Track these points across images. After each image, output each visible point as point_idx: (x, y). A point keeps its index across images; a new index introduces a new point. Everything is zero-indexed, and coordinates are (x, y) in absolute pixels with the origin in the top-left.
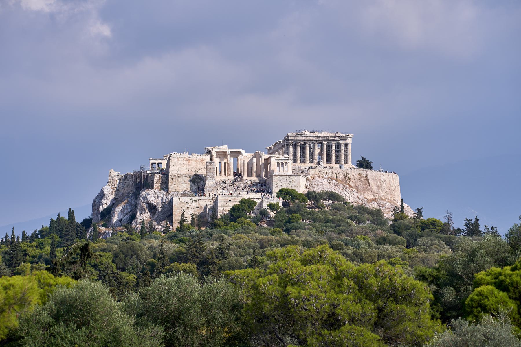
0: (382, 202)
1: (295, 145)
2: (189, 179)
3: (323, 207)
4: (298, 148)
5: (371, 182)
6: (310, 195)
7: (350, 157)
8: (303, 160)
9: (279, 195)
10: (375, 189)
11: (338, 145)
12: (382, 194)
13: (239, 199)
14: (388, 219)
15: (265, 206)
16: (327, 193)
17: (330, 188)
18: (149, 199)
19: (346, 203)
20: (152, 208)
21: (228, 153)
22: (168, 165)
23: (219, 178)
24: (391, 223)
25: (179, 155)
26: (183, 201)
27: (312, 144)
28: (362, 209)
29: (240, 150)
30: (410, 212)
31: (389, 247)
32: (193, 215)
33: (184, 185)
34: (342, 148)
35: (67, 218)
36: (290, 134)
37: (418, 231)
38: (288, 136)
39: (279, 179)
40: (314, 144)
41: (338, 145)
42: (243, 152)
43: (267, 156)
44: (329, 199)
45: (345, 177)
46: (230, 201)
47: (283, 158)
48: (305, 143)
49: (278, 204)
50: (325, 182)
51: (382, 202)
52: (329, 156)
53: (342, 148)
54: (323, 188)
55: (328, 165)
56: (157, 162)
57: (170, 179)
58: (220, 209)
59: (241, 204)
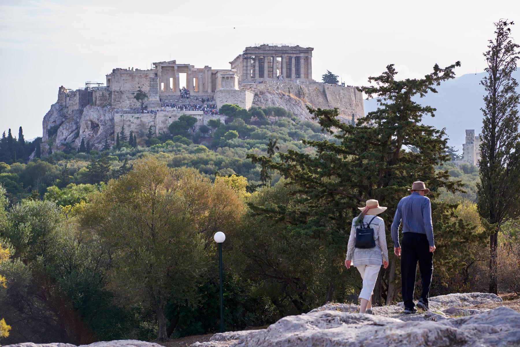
2: (133, 96)
6: (254, 111)
15: (206, 123)
17: (280, 104)
18: (92, 118)
20: (95, 126)
21: (176, 68)
32: (131, 132)
33: (128, 102)
39: (224, 94)
41: (298, 59)
45: (299, 92)
46: (170, 117)
47: (231, 73)
48: (264, 57)
49: (219, 120)
52: (289, 69)
54: (274, 104)
57: (113, 96)
59: (181, 121)
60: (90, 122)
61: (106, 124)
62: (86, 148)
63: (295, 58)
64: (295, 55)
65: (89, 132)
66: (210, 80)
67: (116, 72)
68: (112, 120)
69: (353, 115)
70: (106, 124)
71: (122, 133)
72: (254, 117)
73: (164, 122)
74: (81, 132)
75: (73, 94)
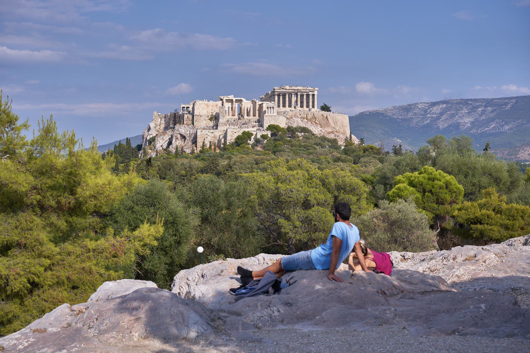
0: (337, 134)
1: (279, 95)
2: (208, 118)
3: (298, 137)
4: (281, 97)
5: (330, 120)
6: (290, 130)
7: (316, 103)
8: (284, 106)
9: (268, 129)
10: (333, 125)
11: (308, 96)
12: (337, 128)
14: (341, 145)
15: (259, 136)
16: (300, 127)
17: (302, 125)
19: (313, 134)
20: (183, 137)
21: (234, 100)
22: (193, 108)
23: (229, 117)
24: (343, 148)
25: (201, 102)
27: (290, 94)
28: (324, 139)
29: (242, 99)
30: (356, 141)
31: (341, 164)
32: (210, 142)
33: (205, 122)
34: (311, 97)
35: (125, 144)
36: (275, 88)
37: (361, 153)
38: (274, 89)
40: (292, 94)
41: (308, 96)
42: (244, 100)
43: (261, 103)
44: (302, 132)
49: (267, 135)
50: (299, 120)
51: (337, 134)
52: (302, 102)
53: (311, 97)
55: (301, 109)
56: (186, 106)
58: (229, 138)
62: (180, 153)
74: (173, 142)
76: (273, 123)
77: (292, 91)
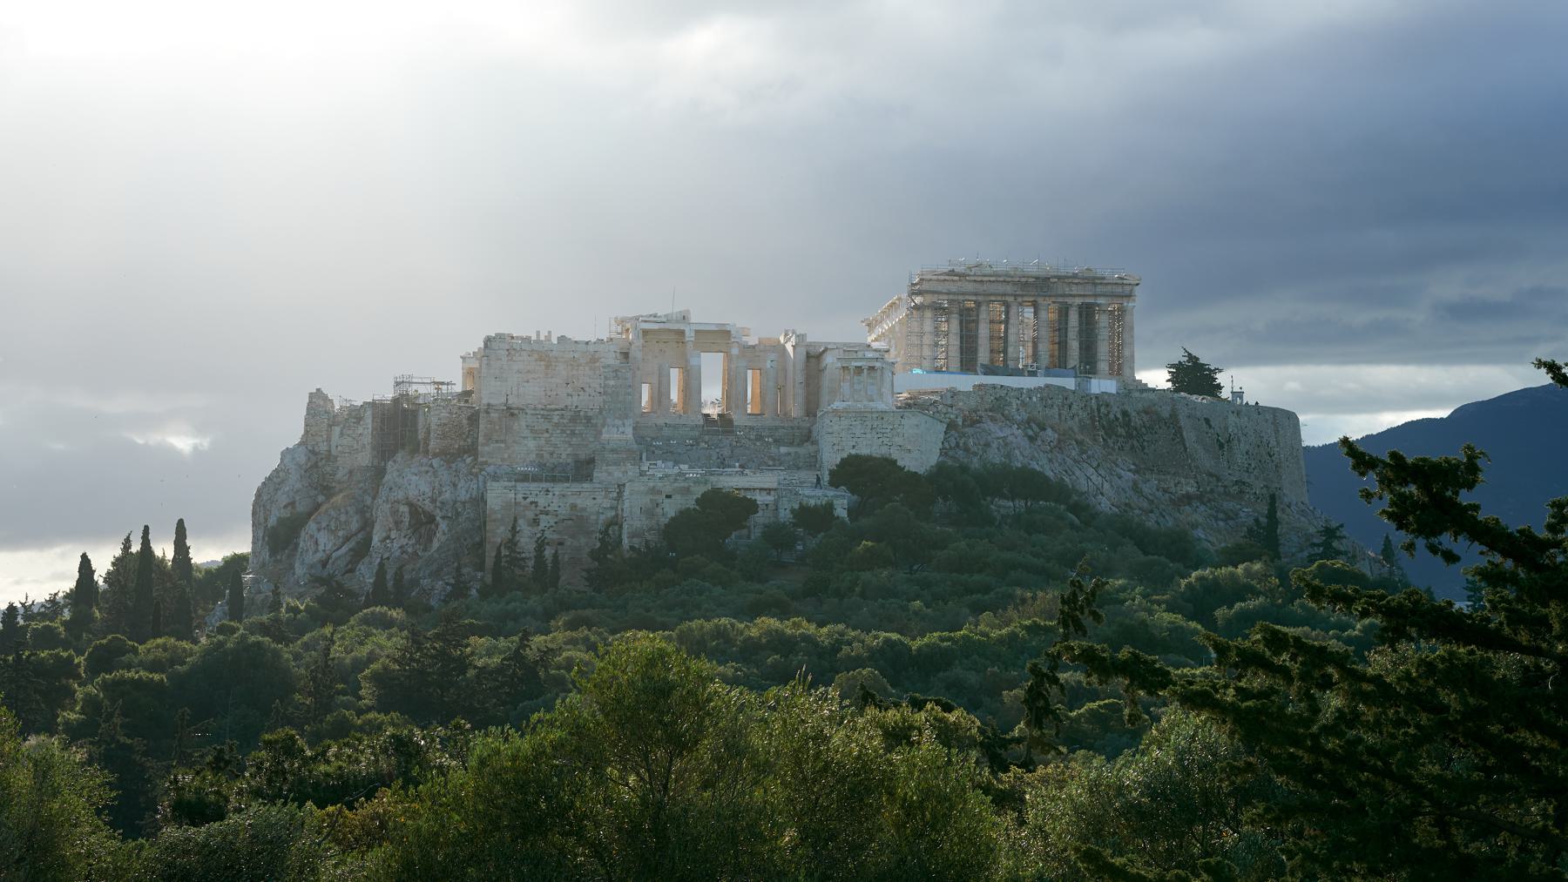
13: (699, 491)
18: (412, 494)
26: (520, 496)
32: (541, 545)
33: (531, 444)
39: (845, 423)
46: (668, 497)
49: (830, 507)
54: (1008, 456)
60: (404, 509)
61: (458, 514)
63: (1080, 307)
64: (1078, 301)
65: (405, 541)
66: (800, 378)
67: (494, 345)
68: (480, 501)
69: (1273, 498)
70: (458, 514)
71: (512, 543)
72: (945, 499)
73: (649, 513)
75: (355, 415)
76: (869, 447)
77: (1009, 289)
